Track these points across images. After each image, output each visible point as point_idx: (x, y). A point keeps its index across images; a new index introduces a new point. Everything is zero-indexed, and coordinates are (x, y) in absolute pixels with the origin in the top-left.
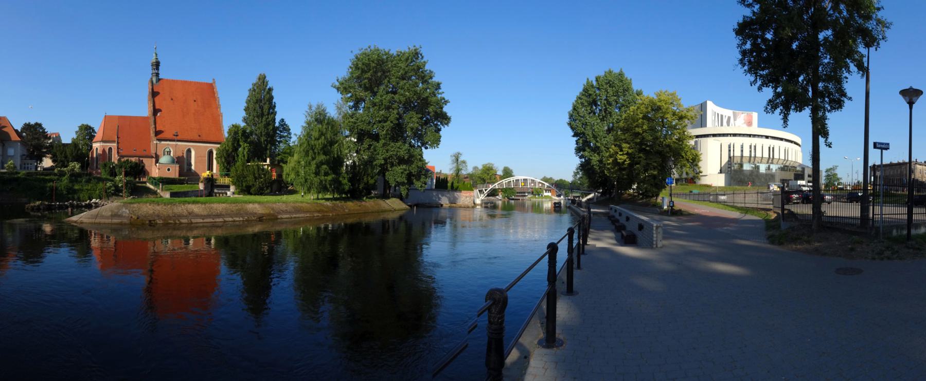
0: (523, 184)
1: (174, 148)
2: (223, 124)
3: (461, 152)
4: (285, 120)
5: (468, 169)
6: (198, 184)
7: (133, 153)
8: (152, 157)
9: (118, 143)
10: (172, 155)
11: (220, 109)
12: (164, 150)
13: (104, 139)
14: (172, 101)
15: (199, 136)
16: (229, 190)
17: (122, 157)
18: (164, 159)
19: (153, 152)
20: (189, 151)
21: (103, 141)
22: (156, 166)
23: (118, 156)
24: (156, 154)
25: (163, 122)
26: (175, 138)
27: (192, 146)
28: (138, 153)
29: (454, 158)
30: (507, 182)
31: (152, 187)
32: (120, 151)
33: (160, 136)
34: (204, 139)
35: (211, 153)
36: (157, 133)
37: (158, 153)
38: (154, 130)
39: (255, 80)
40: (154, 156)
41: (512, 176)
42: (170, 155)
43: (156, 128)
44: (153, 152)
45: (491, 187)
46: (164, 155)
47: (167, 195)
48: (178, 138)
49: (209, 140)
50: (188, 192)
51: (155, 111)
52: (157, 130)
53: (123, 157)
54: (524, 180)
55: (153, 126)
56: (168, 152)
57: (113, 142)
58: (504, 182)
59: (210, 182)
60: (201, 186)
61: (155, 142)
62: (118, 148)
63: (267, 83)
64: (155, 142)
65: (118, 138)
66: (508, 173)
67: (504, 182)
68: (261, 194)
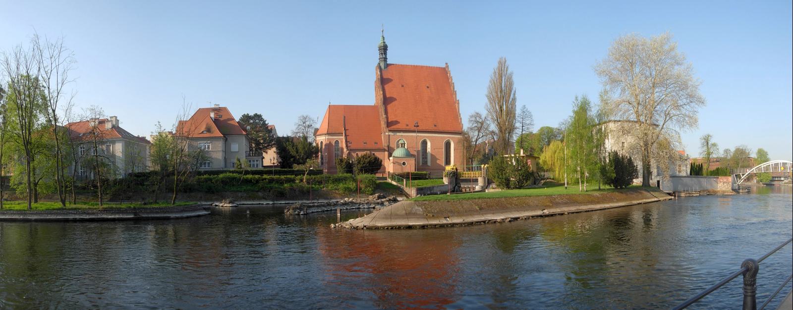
0: (782, 168)
2: (460, 112)
4: (526, 107)
5: (719, 153)
6: (442, 178)
8: (384, 150)
9: (346, 135)
10: (406, 147)
11: (456, 96)
12: (398, 141)
15: (435, 126)
16: (477, 185)
17: (351, 150)
18: (399, 152)
19: (384, 144)
20: (424, 143)
21: (328, 134)
22: (389, 160)
23: (348, 150)
26: (416, 129)
30: (765, 166)
31: (394, 183)
32: (349, 145)
34: (441, 129)
35: (448, 145)
36: (389, 124)
37: (391, 145)
38: (386, 121)
41: (767, 160)
42: (404, 147)
43: (387, 118)
44: (384, 144)
46: (398, 147)
47: (412, 192)
48: (420, 128)
50: (433, 187)
51: (387, 101)
53: (355, 150)
54: (783, 163)
55: (384, 116)
57: (341, 134)
58: (762, 166)
59: (455, 176)
60: (446, 181)
61: (387, 134)
62: (346, 141)
64: (387, 134)
66: (763, 156)
67: (762, 166)
68: (520, 188)
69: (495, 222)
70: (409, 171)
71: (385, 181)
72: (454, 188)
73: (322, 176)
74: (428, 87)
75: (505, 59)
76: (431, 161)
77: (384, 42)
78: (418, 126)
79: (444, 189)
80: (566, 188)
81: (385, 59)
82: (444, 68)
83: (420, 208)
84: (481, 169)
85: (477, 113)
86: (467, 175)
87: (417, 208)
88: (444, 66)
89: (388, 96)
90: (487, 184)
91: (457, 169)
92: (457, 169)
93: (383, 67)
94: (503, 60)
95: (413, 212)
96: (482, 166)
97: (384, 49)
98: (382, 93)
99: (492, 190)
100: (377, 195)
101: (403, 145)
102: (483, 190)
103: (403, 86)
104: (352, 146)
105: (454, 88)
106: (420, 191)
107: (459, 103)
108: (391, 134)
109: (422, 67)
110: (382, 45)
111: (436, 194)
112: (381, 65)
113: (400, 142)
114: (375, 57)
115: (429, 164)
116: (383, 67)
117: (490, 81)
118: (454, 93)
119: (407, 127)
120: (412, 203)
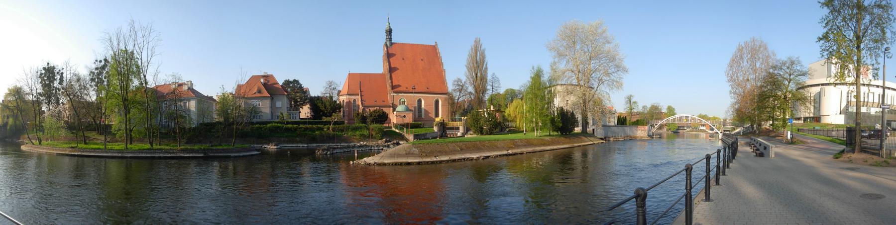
1: (409, 99)
2: (446, 78)
3: (633, 95)
4: (495, 74)
6: (433, 127)
7: (374, 103)
8: (390, 107)
9: (361, 96)
10: (406, 104)
11: (443, 66)
12: (400, 100)
13: (349, 93)
14: (403, 61)
16: (459, 132)
17: (365, 107)
18: (400, 108)
19: (390, 102)
20: (420, 101)
21: (348, 94)
24: (393, 104)
25: (398, 78)
27: (422, 97)
28: (378, 104)
29: (627, 99)
31: (397, 131)
32: (364, 103)
33: (396, 90)
34: (432, 91)
35: (437, 102)
36: (393, 87)
37: (395, 103)
38: (391, 84)
39: (473, 43)
40: (392, 106)
43: (392, 83)
44: (390, 102)
45: (660, 122)
46: (400, 104)
47: (411, 138)
48: (416, 90)
49: (437, 91)
51: (391, 70)
52: (394, 85)
55: (390, 81)
56: (403, 102)
57: (357, 95)
59: (443, 126)
60: (436, 129)
62: (362, 100)
63: (481, 45)
64: (392, 94)
65: (361, 91)
66: (671, 111)
68: (491, 134)
69: (472, 159)
70: (408, 122)
71: (390, 129)
72: (442, 134)
73: (344, 125)
74: (422, 60)
75: (479, 39)
76: (425, 115)
77: (390, 27)
78: (414, 89)
79: (434, 135)
80: (525, 134)
81: (390, 39)
82: (434, 46)
83: (417, 150)
84: (461, 121)
85: (459, 79)
86: (451, 124)
87: (414, 149)
88: (434, 44)
89: (392, 66)
90: (466, 131)
91: (443, 120)
92: (443, 120)
93: (389, 45)
94: (478, 39)
95: (411, 152)
96: (463, 118)
97: (389, 32)
98: (388, 64)
99: (469, 136)
100: (384, 139)
101: (403, 103)
102: (463, 135)
103: (403, 59)
104: (366, 104)
105: (441, 61)
106: (417, 137)
107: (445, 72)
108: (395, 94)
109: (418, 45)
110: (388, 28)
111: (428, 139)
112: (387, 43)
113: (402, 100)
114: (383, 37)
115: (423, 116)
116: (389, 45)
117: (469, 55)
118: (441, 64)
119: (407, 90)
120: (410, 146)
